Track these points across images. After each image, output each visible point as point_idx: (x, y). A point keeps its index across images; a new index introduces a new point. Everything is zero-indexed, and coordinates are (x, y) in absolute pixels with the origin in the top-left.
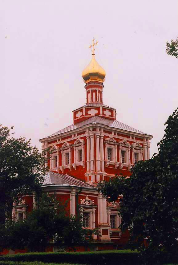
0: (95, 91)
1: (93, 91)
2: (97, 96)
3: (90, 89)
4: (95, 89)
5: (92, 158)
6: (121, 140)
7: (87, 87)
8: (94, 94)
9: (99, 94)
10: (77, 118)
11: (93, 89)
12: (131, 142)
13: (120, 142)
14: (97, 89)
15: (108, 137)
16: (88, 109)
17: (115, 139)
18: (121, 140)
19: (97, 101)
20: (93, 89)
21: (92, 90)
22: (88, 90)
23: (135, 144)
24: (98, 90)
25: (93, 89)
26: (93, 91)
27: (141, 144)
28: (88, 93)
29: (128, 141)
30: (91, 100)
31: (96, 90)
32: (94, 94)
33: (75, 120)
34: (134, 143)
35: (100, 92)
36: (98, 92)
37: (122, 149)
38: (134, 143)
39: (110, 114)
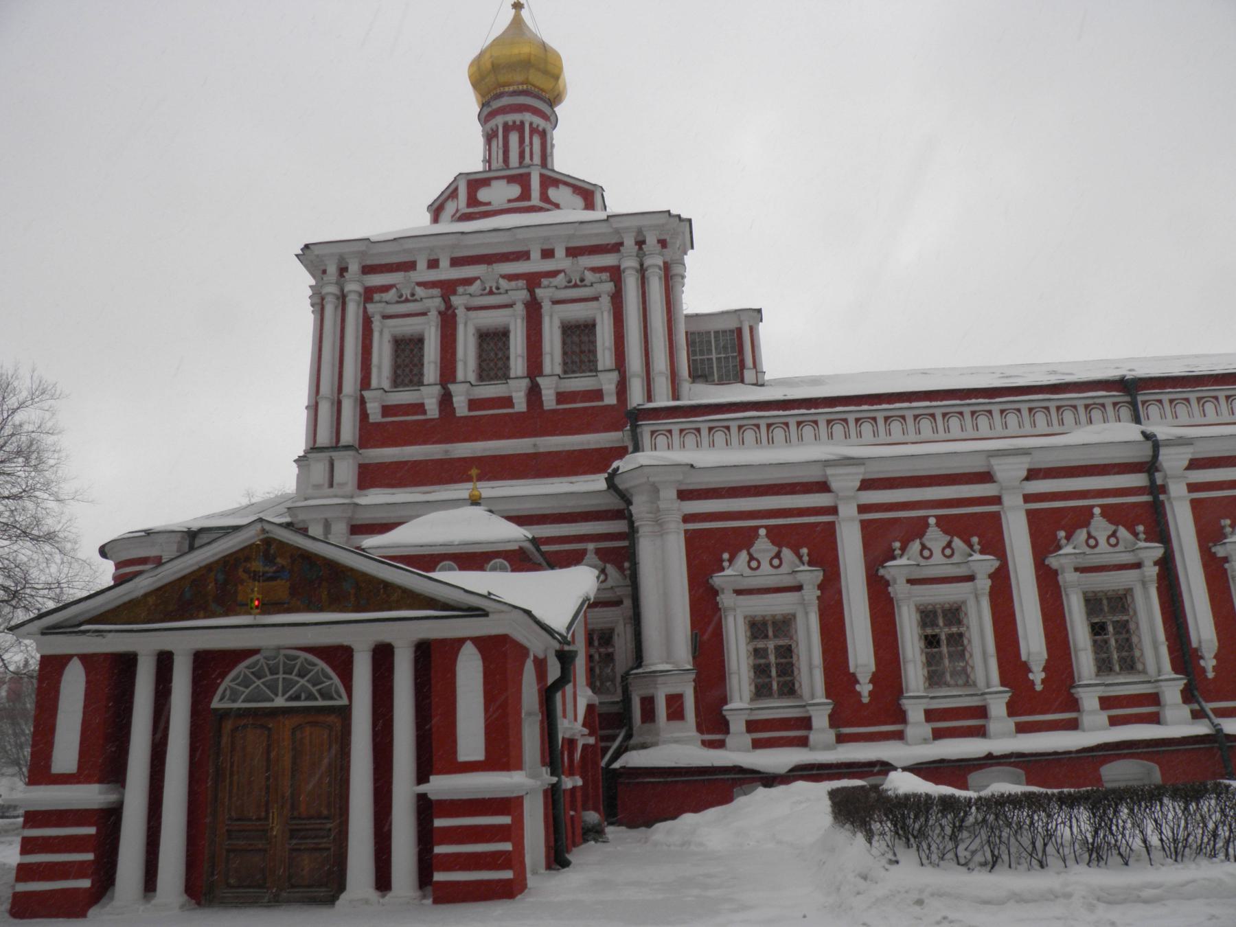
0: (520, 128)
1: (507, 128)
3: (499, 120)
7: (485, 118)
8: (514, 138)
9: (537, 141)
11: (510, 118)
14: (528, 117)
16: (475, 183)
20: (510, 123)
22: (492, 123)
24: (531, 124)
25: (510, 123)
28: (490, 137)
31: (522, 123)
32: (514, 138)
35: (543, 135)
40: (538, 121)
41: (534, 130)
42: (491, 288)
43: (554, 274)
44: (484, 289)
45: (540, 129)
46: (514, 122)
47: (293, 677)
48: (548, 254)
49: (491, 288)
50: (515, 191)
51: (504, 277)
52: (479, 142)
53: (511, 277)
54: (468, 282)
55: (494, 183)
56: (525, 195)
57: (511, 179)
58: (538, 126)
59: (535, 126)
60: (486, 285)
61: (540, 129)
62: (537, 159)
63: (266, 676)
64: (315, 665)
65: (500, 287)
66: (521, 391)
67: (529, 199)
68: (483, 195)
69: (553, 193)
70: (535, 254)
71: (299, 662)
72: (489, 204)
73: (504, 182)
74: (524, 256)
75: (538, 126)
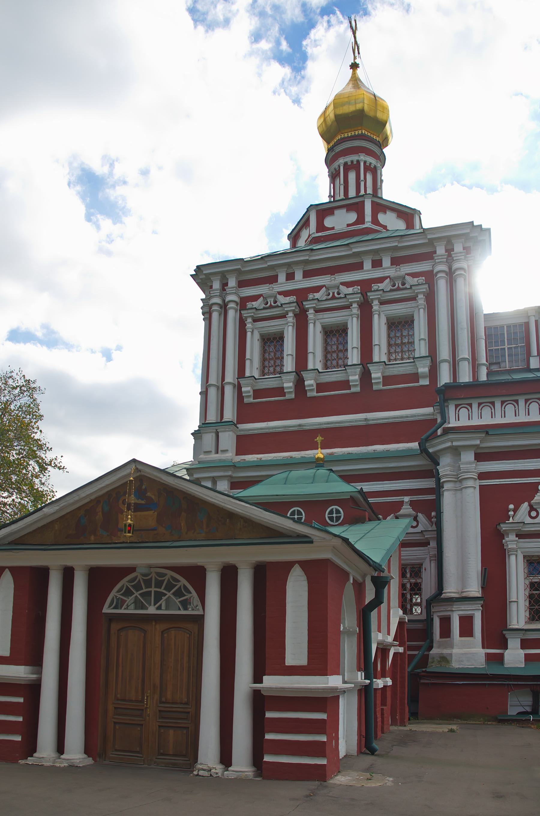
0: (355, 166)
1: (347, 168)
2: (362, 178)
3: (341, 161)
7: (329, 161)
8: (352, 176)
11: (349, 159)
14: (363, 157)
20: (349, 164)
21: (345, 164)
22: (335, 165)
24: (365, 162)
25: (349, 164)
26: (347, 168)
28: (333, 176)
31: (358, 162)
32: (352, 176)
40: (371, 160)
41: (367, 168)
42: (333, 293)
43: (381, 280)
44: (329, 294)
45: (372, 167)
46: (352, 162)
47: (162, 590)
48: (377, 264)
49: (333, 293)
50: (353, 217)
51: (343, 284)
52: (326, 180)
53: (348, 284)
54: (317, 289)
55: (336, 212)
56: (361, 220)
57: (349, 208)
58: (370, 164)
59: (368, 164)
60: (330, 291)
62: (370, 191)
63: (142, 589)
64: (178, 581)
65: (340, 292)
66: (356, 375)
67: (363, 222)
68: (328, 222)
69: (381, 217)
70: (368, 265)
71: (166, 578)
72: (333, 228)
73: (344, 210)
74: (359, 266)
75: (370, 164)
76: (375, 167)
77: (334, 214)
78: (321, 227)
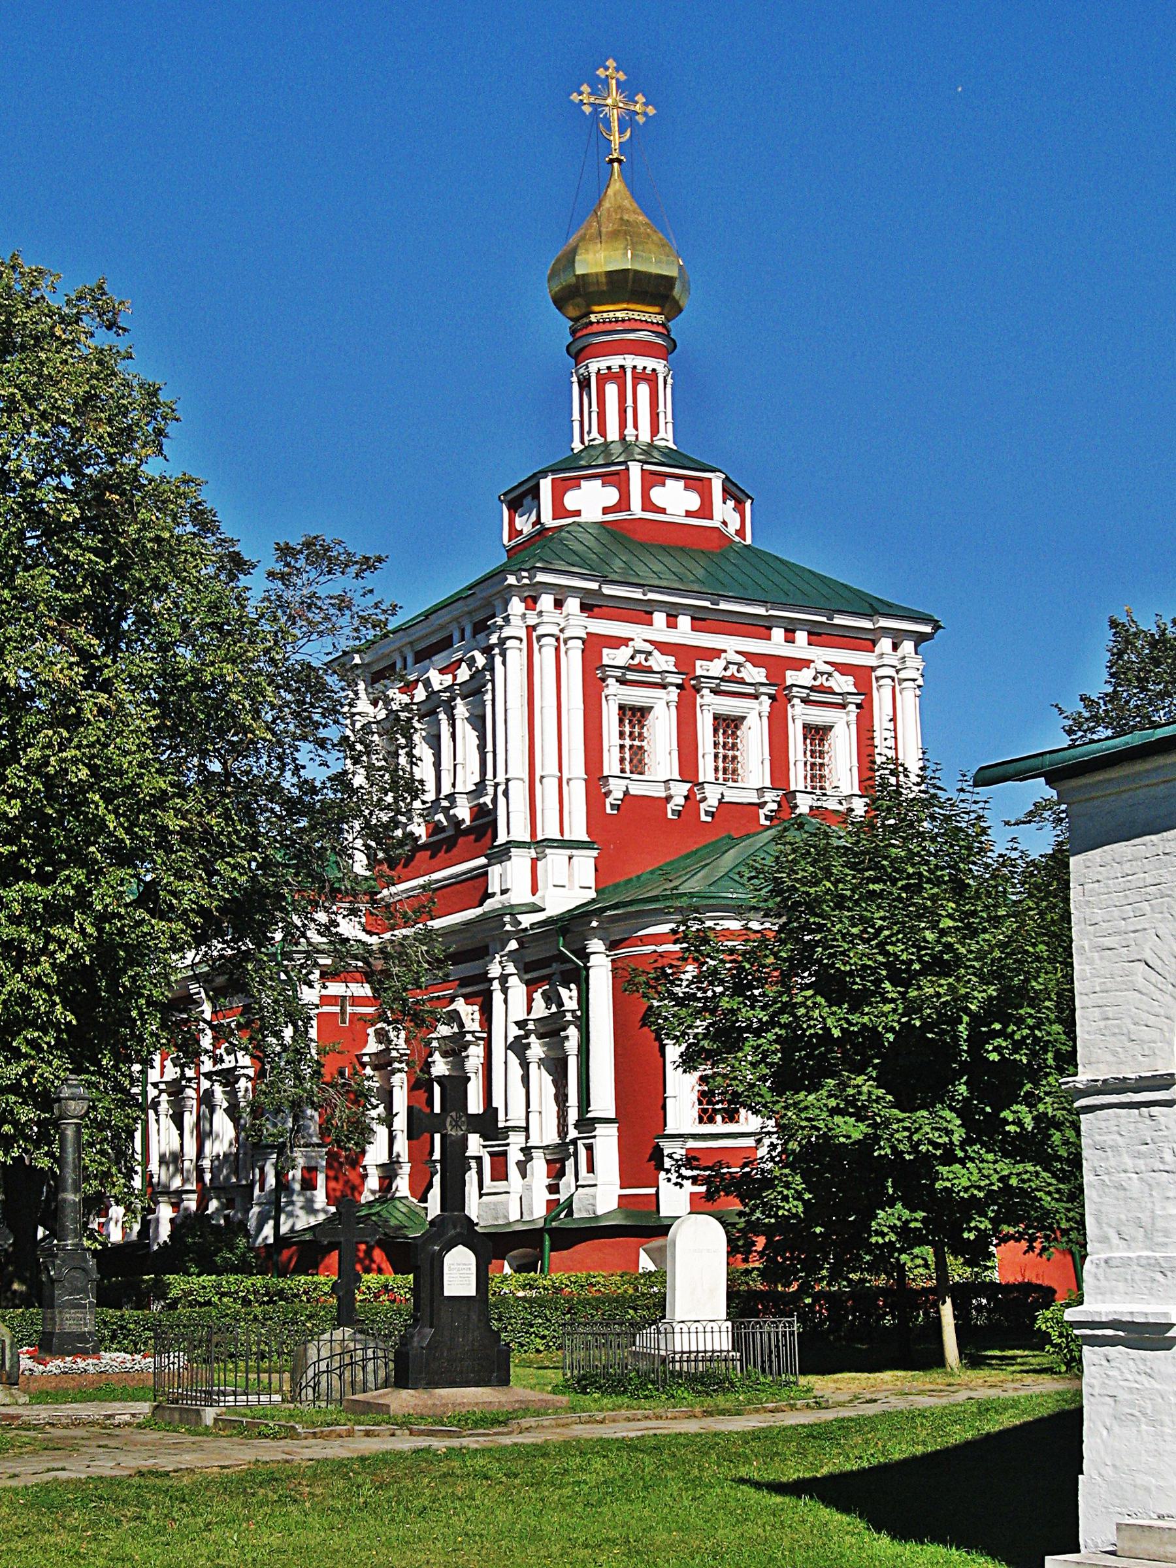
0: (618, 376)
1: (603, 379)
4: (615, 362)
5: (519, 768)
6: (713, 654)
8: (611, 390)
9: (643, 390)
10: (521, 532)
12: (776, 666)
13: (701, 668)
14: (629, 361)
15: (618, 642)
17: (664, 648)
18: (713, 654)
19: (630, 430)
21: (599, 370)
23: (804, 677)
27: (844, 669)
29: (755, 659)
30: (595, 433)
32: (611, 390)
33: (512, 543)
34: (801, 664)
36: (634, 378)
37: (709, 705)
38: (801, 664)
39: (693, 501)
41: (639, 377)
45: (648, 371)
50: (611, 495)
58: (645, 368)
59: (640, 368)
61: (648, 371)
68: (571, 500)
75: (645, 368)
76: (654, 370)
77: (579, 486)
78: (559, 510)
